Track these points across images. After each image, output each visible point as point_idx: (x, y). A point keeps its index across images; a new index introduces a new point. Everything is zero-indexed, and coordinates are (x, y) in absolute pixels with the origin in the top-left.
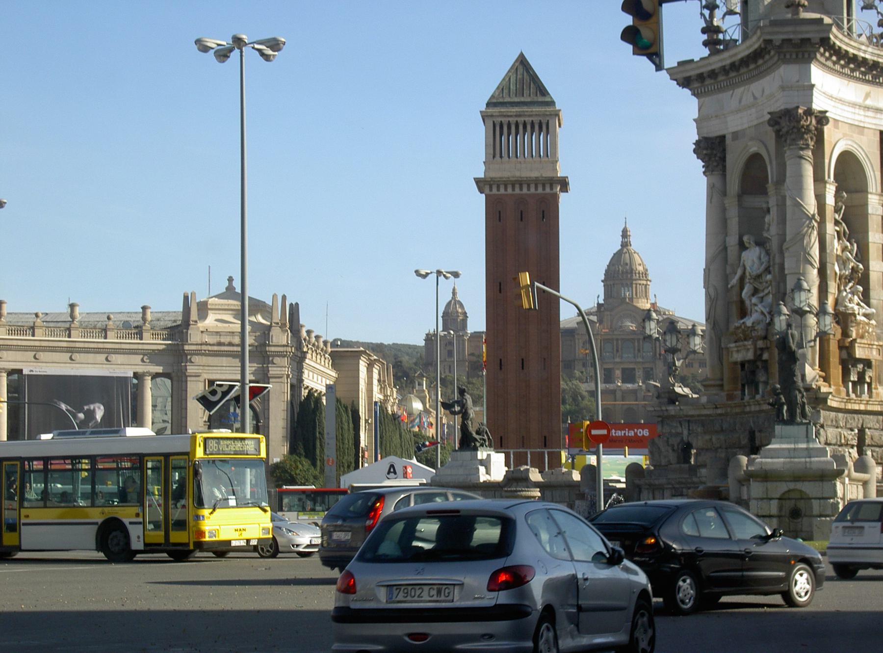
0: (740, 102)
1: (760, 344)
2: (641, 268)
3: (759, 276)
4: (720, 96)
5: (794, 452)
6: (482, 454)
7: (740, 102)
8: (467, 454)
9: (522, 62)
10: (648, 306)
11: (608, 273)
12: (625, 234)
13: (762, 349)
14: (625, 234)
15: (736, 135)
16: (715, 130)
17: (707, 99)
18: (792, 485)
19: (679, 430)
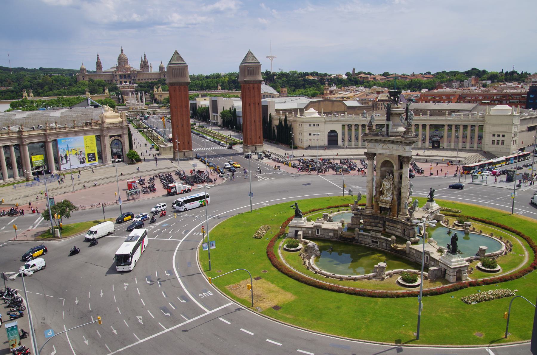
0: (382, 147)
1: (390, 204)
2: (126, 58)
3: (388, 189)
4: (375, 144)
5: (458, 261)
6: (303, 218)
7: (382, 147)
8: (299, 218)
9: (176, 53)
10: (128, 67)
11: (118, 59)
12: (122, 50)
13: (390, 206)
14: (122, 50)
15: (380, 154)
16: (373, 151)
17: (370, 143)
18: (459, 269)
19: (360, 217)
